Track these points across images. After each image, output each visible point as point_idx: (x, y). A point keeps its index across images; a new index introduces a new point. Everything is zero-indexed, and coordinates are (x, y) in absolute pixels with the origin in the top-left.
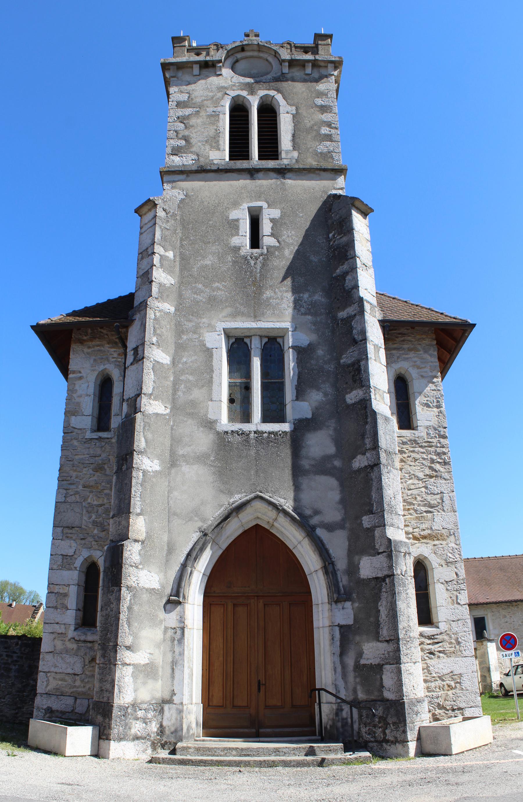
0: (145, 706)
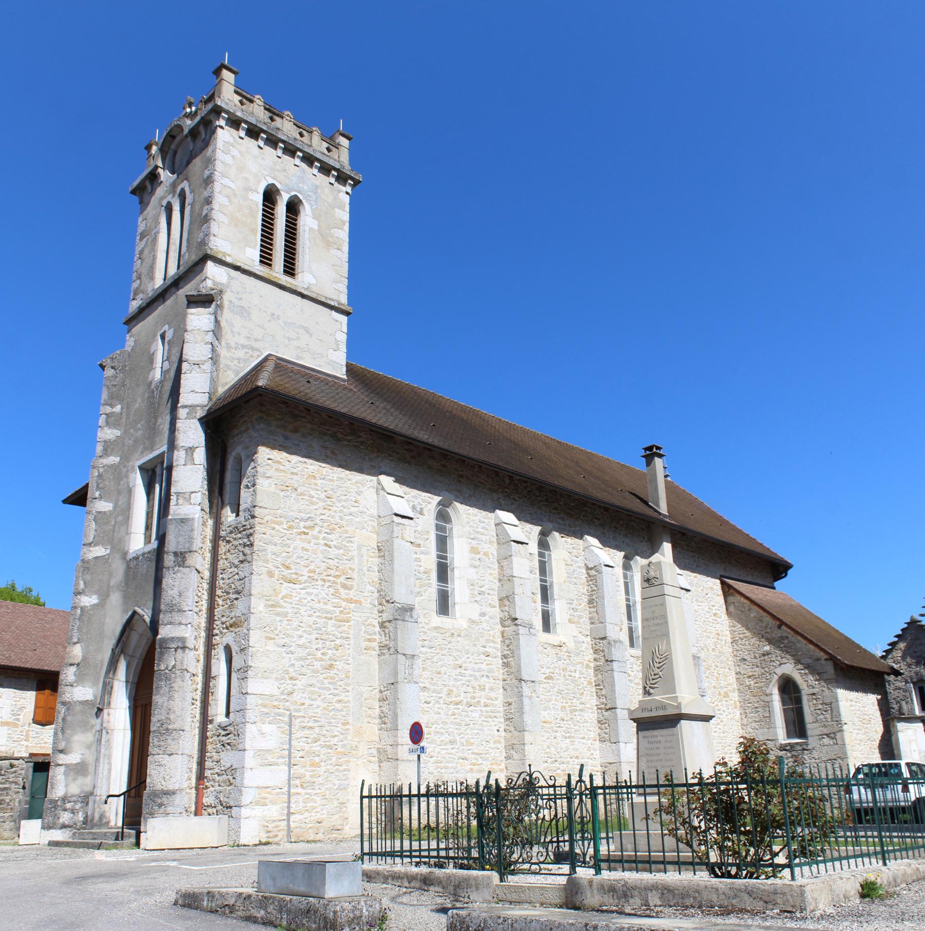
0: (72, 799)
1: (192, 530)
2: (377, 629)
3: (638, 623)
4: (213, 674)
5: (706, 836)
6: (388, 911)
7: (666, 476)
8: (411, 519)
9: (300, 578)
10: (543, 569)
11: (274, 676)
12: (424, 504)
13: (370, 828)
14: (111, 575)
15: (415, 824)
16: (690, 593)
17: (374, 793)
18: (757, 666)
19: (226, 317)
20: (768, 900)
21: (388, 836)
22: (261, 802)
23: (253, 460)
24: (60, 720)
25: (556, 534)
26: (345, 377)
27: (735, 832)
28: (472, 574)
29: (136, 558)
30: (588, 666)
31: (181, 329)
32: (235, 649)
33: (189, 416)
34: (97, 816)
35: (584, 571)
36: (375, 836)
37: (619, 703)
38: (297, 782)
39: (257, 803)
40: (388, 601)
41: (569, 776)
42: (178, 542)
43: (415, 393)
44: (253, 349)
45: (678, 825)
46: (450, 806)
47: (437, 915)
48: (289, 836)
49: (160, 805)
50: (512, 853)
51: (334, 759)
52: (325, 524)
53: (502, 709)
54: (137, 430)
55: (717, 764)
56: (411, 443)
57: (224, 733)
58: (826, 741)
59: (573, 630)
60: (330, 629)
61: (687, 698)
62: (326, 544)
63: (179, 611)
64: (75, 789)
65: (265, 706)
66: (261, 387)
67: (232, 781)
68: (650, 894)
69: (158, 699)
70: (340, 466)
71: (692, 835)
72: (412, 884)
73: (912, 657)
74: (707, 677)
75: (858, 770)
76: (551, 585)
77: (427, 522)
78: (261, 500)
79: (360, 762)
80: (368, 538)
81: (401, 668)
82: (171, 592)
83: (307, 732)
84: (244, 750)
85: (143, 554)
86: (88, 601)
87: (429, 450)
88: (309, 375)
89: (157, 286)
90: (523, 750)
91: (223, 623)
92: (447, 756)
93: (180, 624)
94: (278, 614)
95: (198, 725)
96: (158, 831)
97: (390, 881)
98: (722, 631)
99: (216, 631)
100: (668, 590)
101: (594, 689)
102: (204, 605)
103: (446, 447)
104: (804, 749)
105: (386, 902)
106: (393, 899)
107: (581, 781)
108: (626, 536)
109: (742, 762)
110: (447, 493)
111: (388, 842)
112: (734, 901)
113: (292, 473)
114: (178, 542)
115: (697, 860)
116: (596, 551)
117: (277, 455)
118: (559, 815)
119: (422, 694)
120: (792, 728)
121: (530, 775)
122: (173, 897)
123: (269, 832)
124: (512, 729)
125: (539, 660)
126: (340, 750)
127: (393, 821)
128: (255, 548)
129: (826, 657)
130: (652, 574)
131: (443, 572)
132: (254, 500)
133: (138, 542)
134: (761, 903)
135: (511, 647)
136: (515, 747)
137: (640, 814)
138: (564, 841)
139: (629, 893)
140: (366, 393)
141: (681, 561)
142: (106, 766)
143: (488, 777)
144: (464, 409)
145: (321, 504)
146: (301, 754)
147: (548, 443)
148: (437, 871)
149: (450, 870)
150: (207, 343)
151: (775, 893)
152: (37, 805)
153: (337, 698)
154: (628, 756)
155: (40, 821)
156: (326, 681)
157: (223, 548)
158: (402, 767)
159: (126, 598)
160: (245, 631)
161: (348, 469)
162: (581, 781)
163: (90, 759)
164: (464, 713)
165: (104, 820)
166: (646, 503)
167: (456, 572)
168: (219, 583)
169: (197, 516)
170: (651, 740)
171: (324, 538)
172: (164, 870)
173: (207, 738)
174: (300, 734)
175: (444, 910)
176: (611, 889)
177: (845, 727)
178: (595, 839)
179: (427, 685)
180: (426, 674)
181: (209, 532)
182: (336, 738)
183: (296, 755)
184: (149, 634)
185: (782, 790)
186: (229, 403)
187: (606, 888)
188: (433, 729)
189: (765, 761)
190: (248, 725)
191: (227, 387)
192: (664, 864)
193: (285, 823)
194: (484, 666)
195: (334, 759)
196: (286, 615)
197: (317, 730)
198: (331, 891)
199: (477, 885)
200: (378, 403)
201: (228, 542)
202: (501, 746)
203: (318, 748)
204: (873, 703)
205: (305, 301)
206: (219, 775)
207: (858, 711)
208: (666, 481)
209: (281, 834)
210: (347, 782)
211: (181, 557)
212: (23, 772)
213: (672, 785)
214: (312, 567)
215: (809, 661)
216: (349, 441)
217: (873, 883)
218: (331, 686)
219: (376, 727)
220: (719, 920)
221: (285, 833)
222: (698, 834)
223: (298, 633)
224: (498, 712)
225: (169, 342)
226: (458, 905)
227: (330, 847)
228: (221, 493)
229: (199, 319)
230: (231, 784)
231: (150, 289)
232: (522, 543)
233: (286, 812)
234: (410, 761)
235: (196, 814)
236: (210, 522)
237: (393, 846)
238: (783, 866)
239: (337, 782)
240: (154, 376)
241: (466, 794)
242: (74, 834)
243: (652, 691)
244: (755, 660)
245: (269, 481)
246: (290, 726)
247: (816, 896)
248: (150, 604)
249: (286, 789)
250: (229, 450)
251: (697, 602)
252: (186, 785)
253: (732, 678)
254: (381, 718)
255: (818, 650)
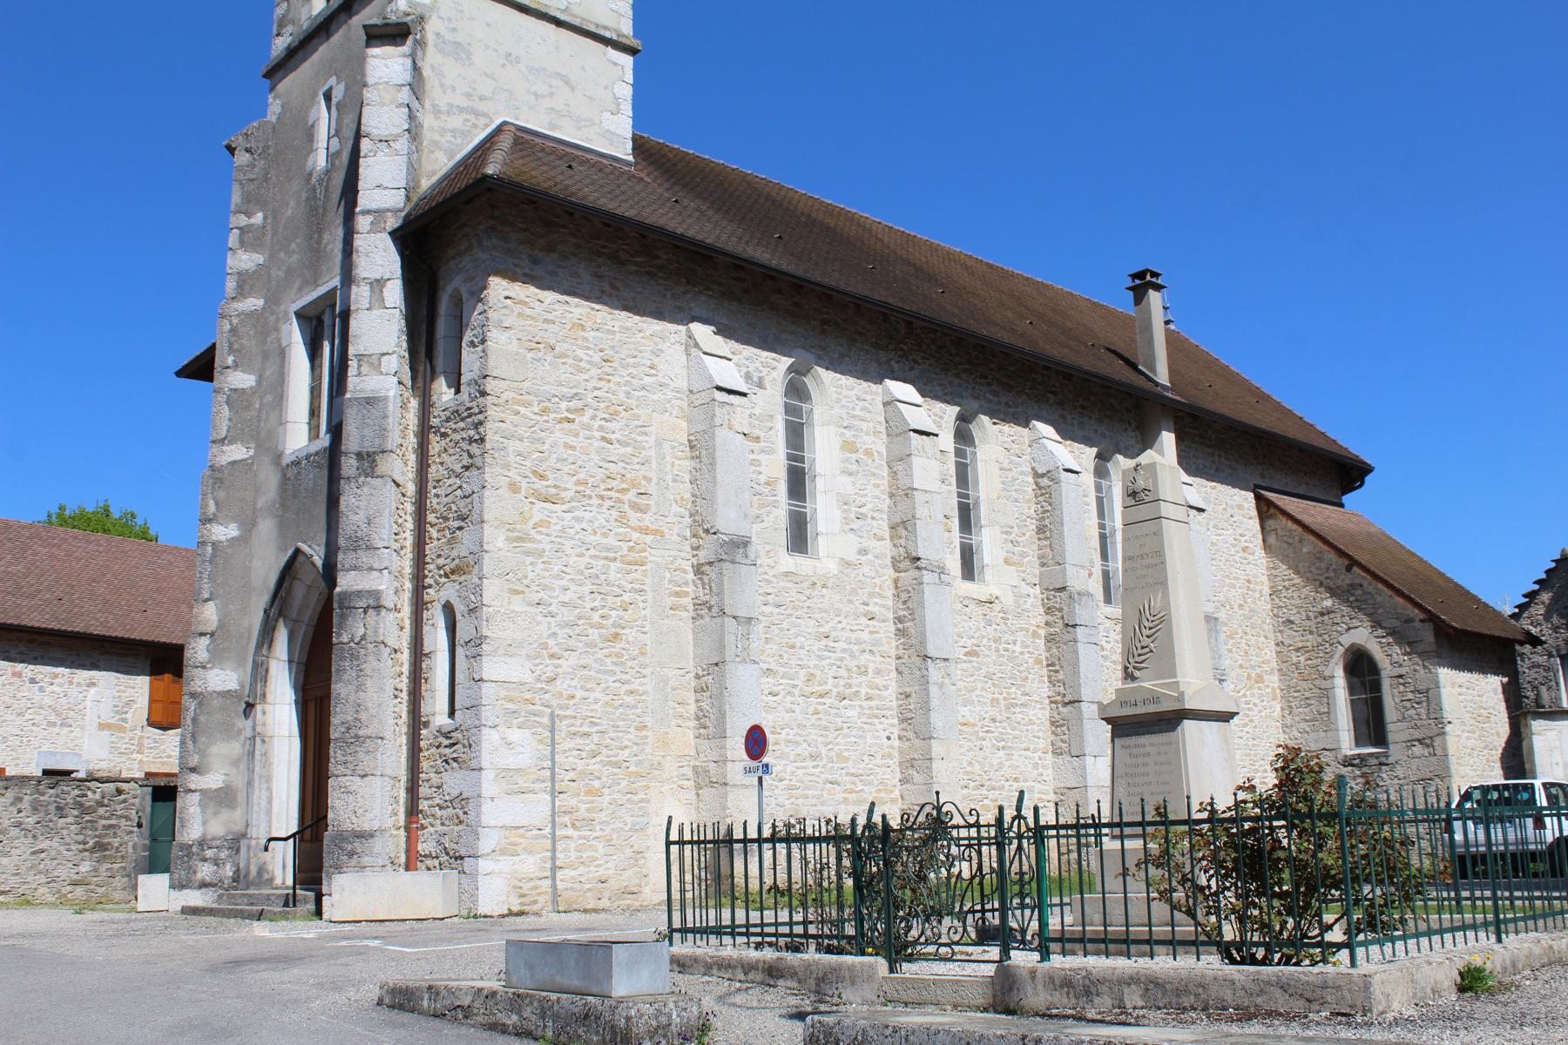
0: (214, 843)
1: (385, 417)
2: (691, 576)
3: (1117, 564)
4: (426, 650)
5: (1219, 902)
6: (711, 1017)
7: (1167, 323)
8: (744, 395)
9: (563, 494)
10: (963, 476)
11: (524, 652)
12: (765, 371)
13: (683, 891)
14: (257, 490)
15: (754, 885)
16: (1204, 515)
17: (687, 837)
18: (1311, 633)
19: (432, 59)
20: (1312, 997)
21: (712, 902)
22: (509, 851)
23: (481, 300)
24: (189, 722)
25: (985, 419)
26: (631, 158)
27: (1264, 894)
28: (845, 485)
29: (296, 463)
30: (1035, 635)
31: (357, 83)
32: (459, 609)
33: (375, 228)
34: (254, 871)
35: (1031, 480)
36: (689, 902)
37: (1086, 694)
38: (566, 819)
39: (503, 852)
40: (707, 531)
41: (1001, 809)
42: (363, 437)
43: (749, 184)
44: (477, 114)
45: (1174, 883)
46: (810, 856)
47: (789, 1022)
48: (555, 902)
49: (351, 854)
50: (909, 928)
51: (624, 783)
52: (603, 405)
53: (894, 704)
54: (290, 254)
55: (1240, 788)
56: (742, 268)
57: (446, 742)
58: (1418, 750)
59: (1011, 576)
60: (613, 576)
61: (1193, 683)
62: (603, 438)
63: (368, 548)
64: (217, 828)
65: (511, 700)
66: (491, 177)
67: (462, 817)
68: (1126, 991)
69: (339, 688)
70: (625, 308)
71: (1195, 899)
72: (750, 977)
73: (1561, 616)
74: (1230, 651)
75: (1466, 796)
76: (977, 503)
77: (772, 398)
78: (496, 365)
79: (666, 787)
80: (672, 427)
81: (730, 639)
82: (354, 518)
83: (579, 741)
84: (480, 769)
85: (308, 457)
86: (223, 532)
87: (773, 278)
88: (571, 156)
89: (315, 12)
90: (930, 768)
91: (439, 568)
92: (806, 779)
93: (371, 569)
94: (528, 553)
95: (404, 729)
96: (348, 893)
97: (715, 971)
98: (1255, 576)
99: (428, 581)
100: (1166, 510)
101: (1045, 672)
102: (408, 538)
103: (800, 272)
104: (1381, 764)
105: (708, 1003)
106: (721, 999)
107: (1019, 816)
108: (1100, 421)
109: (1280, 786)
110: (801, 352)
111: (712, 912)
112: (1259, 1000)
113: (546, 321)
114: (363, 437)
115: (1203, 938)
116: (1051, 445)
117: (519, 290)
118: (986, 870)
119: (764, 680)
120: (1364, 730)
121: (938, 808)
122: (375, 993)
123: (523, 896)
124: (911, 735)
125: (955, 626)
126: (632, 769)
127: (718, 878)
128: (488, 445)
129: (1422, 616)
130: (1141, 483)
131: (798, 482)
132: (484, 366)
133: (297, 438)
134: (1302, 1002)
135: (909, 604)
136: (916, 763)
137: (1113, 867)
138: (993, 910)
139: (1093, 989)
140: (667, 185)
141: (1190, 461)
142: (264, 793)
143: (871, 811)
144: (829, 210)
145: (595, 372)
146: (571, 775)
147: (970, 266)
148: (790, 957)
149: (811, 955)
150: (400, 105)
151: (1324, 987)
152: (160, 854)
153: (627, 687)
154: (1096, 778)
155: (167, 876)
156: (608, 660)
157: (435, 445)
158: (733, 795)
159: (283, 527)
160: (475, 580)
161: (637, 313)
162: (1019, 816)
163: (239, 782)
164: (833, 711)
165: (266, 876)
166: (1134, 366)
167: (819, 482)
168: (432, 502)
169: (391, 393)
170: (1135, 751)
171: (601, 428)
172: (362, 952)
173: (420, 750)
174: (567, 745)
175: (800, 1016)
176: (1065, 983)
177: (1448, 728)
178: (1040, 907)
179: (773, 666)
180: (772, 648)
181: (412, 419)
182: (627, 751)
183: (561, 774)
184: (323, 585)
185: (1341, 829)
186: (439, 205)
187: (1057, 982)
188: (783, 736)
189: (1317, 783)
190: (485, 731)
191: (435, 179)
192: (1150, 944)
193: (549, 882)
194: (865, 636)
195: (624, 783)
196: (541, 553)
197: (596, 738)
198: (621, 986)
199: (854, 978)
200: (685, 202)
201: (444, 435)
202: (894, 763)
203: (597, 767)
204: (1495, 690)
205: (562, 31)
206: (441, 808)
207: (1471, 702)
208: (1167, 331)
209: (541, 899)
210: (645, 820)
211: (369, 461)
212: (137, 801)
213: (1166, 823)
214: (582, 476)
215: (1395, 623)
216: (638, 264)
217: (1479, 970)
218: (617, 669)
219: (691, 734)
220: (1235, 1029)
221: (549, 898)
222: (1206, 898)
223: (562, 583)
224: (890, 709)
225: (338, 105)
226: (823, 1008)
227: (620, 919)
228: (430, 355)
229: (386, 64)
230: (461, 822)
231: (304, 17)
232: (928, 434)
233: (549, 865)
234: (747, 787)
235: (407, 868)
236: (414, 404)
237: (719, 918)
238: (1339, 946)
239: (629, 820)
240: (315, 164)
241: (836, 837)
242: (220, 896)
243: (1137, 674)
244: (1308, 623)
245: (508, 333)
246: (552, 731)
247: (1388, 990)
248: (322, 538)
249: (548, 830)
250: (441, 283)
251: (1216, 533)
252: (389, 822)
253: (1270, 653)
254: (698, 718)
255: (1410, 606)
